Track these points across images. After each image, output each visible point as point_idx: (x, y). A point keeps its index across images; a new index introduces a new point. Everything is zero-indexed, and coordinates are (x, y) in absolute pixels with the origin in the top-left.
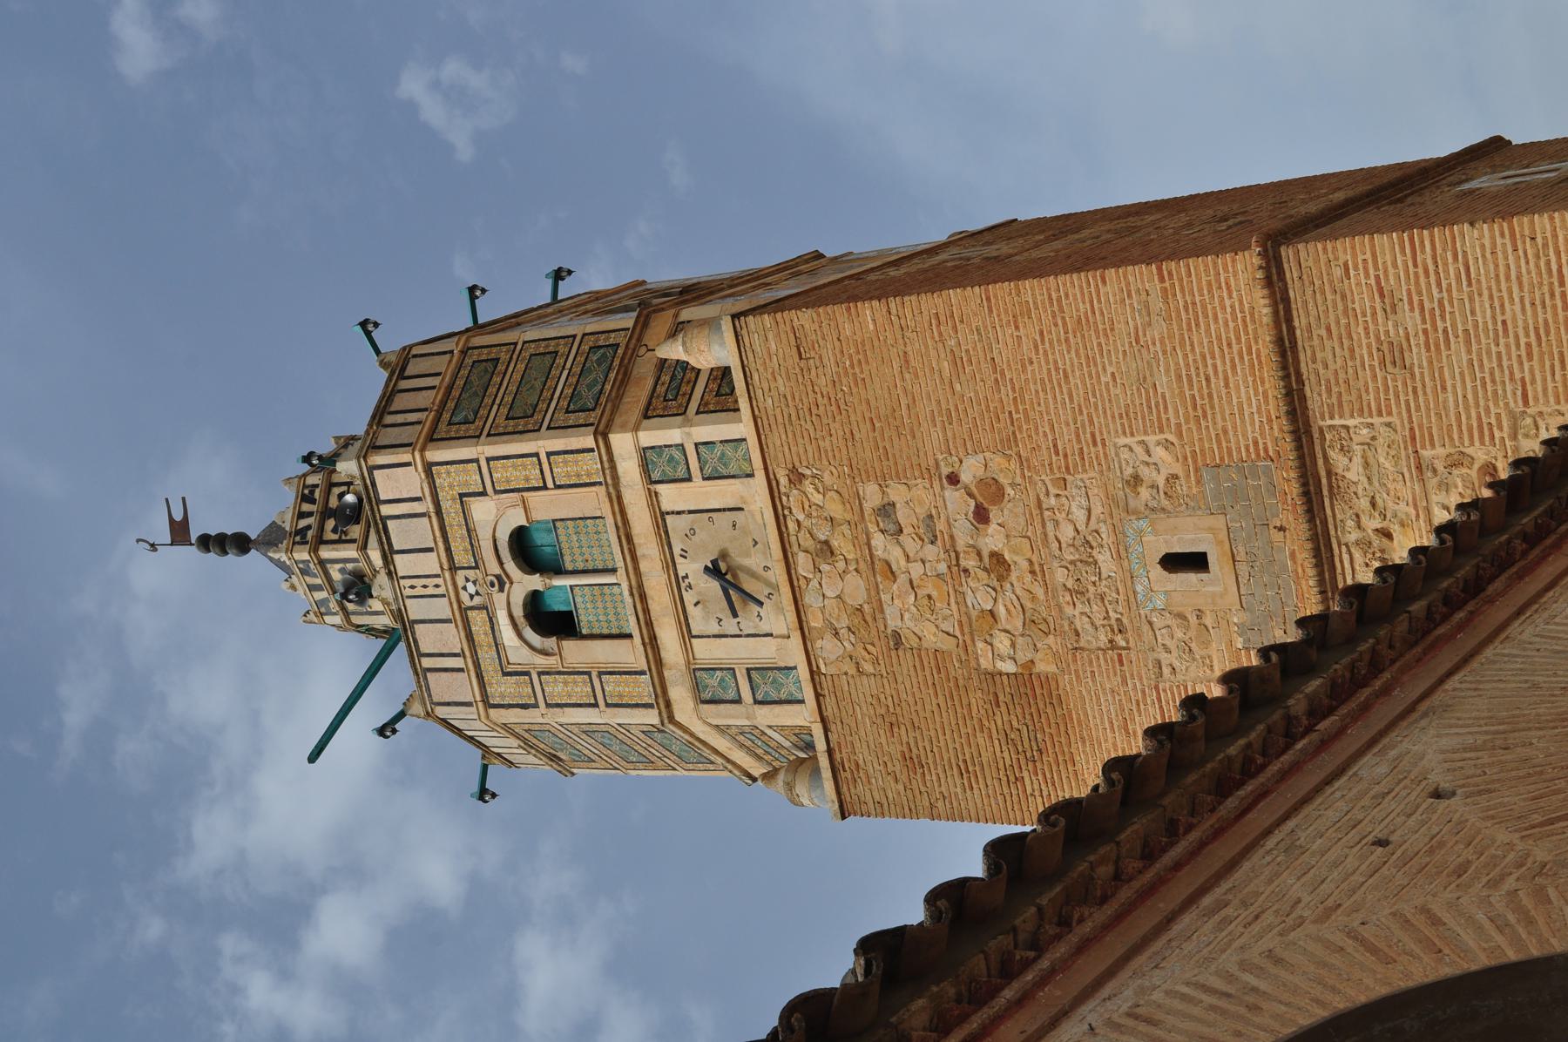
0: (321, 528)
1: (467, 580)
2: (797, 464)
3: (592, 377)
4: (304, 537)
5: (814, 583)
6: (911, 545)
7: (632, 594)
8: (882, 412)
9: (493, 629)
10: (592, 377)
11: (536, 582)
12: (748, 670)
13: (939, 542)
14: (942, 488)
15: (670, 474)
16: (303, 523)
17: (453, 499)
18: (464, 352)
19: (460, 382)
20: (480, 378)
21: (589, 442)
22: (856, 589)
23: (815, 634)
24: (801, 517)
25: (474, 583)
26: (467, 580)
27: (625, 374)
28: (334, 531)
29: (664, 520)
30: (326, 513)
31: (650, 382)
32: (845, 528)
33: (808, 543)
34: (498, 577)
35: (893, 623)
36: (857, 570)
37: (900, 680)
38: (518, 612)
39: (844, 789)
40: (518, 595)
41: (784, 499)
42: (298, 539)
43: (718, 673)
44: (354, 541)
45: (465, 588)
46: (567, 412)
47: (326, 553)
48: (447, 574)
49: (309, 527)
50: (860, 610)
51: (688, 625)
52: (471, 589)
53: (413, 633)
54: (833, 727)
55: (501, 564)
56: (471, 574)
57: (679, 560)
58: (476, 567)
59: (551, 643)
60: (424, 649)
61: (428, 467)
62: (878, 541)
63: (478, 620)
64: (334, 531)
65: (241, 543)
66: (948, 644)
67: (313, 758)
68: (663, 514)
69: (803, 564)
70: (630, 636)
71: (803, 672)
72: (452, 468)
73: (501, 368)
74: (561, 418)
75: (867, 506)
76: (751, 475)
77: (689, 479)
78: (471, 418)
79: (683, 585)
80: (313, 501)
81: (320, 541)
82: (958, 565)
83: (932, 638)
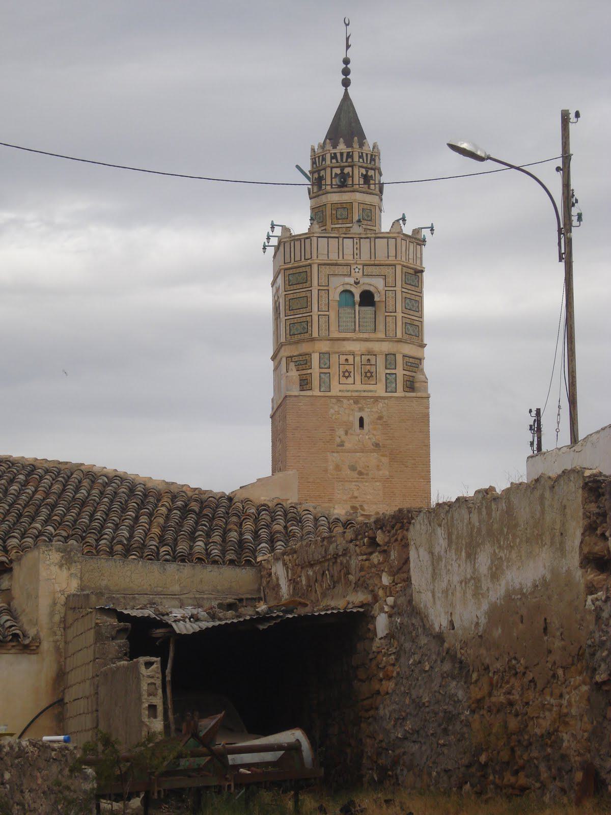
1: (359, 269)
26: (359, 269)
30: (367, 169)
34: (359, 283)
38: (348, 288)
40: (353, 289)
42: (360, 154)
45: (357, 268)
48: (362, 262)
56: (361, 271)
63: (345, 270)
65: (346, 83)
68: (376, 355)
80: (370, 163)
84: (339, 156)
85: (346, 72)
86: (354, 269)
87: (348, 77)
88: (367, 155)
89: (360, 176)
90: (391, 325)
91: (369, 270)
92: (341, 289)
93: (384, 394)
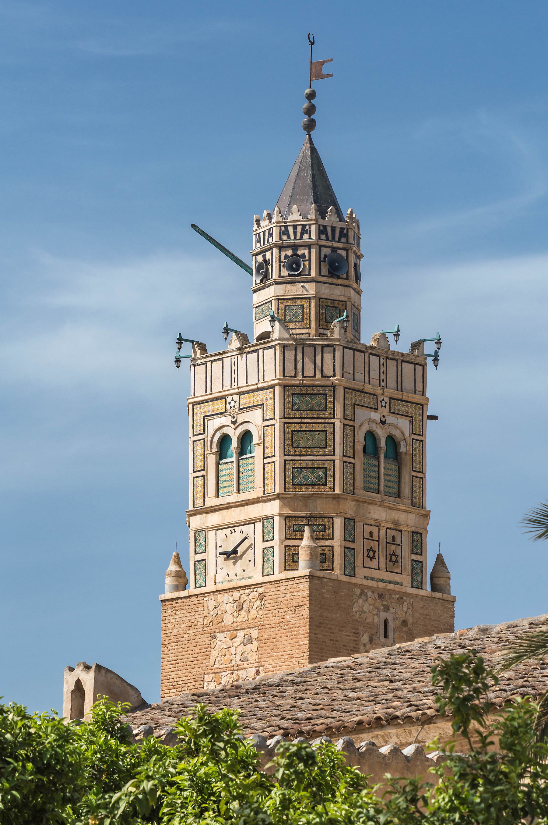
0: (287, 247)
2: (265, 598)
3: (311, 476)
4: (284, 234)
5: (231, 600)
6: (240, 649)
7: (228, 503)
8: (278, 643)
9: (218, 414)
10: (311, 476)
11: (234, 445)
12: (205, 560)
13: (241, 663)
14: (256, 667)
15: (266, 531)
16: (291, 229)
17: (262, 400)
18: (333, 386)
19: (315, 391)
20: (316, 404)
21: (277, 491)
22: (228, 620)
23: (216, 596)
24: (250, 597)
25: (234, 407)
26: (235, 402)
27: (308, 497)
28: (286, 257)
29: (252, 523)
30: (295, 247)
31: (303, 514)
32: (246, 618)
33: (242, 600)
35: (218, 635)
36: (234, 622)
37: (202, 636)
38: (225, 431)
39: (170, 603)
41: (255, 590)
42: (283, 229)
43: (204, 544)
44: (280, 276)
46: (293, 468)
47: (275, 250)
48: (236, 391)
49: (289, 237)
50: (222, 621)
51: (219, 529)
52: (233, 404)
53: (219, 359)
54: (188, 600)
55: (241, 424)
56: (237, 405)
57: (240, 528)
58: (240, 409)
59: (215, 449)
60: (213, 363)
61: (273, 387)
62: (241, 634)
63: (220, 406)
64: (286, 257)
66: (212, 659)
67: (193, 226)
69: (236, 594)
70: (217, 495)
71: (203, 590)
72: (272, 402)
73: (321, 414)
74: (290, 466)
75: (251, 630)
76: (263, 576)
77: (264, 541)
78: (296, 407)
79: (232, 529)
80: (301, 237)
81: (281, 248)
82: (234, 670)
83: (214, 653)
84: (329, 229)
85: (310, 111)
86: (230, 403)
87: (312, 117)
88: (295, 227)
89: (282, 259)
90: (270, 475)
91: (246, 400)
92: (218, 435)
93: (261, 579)
